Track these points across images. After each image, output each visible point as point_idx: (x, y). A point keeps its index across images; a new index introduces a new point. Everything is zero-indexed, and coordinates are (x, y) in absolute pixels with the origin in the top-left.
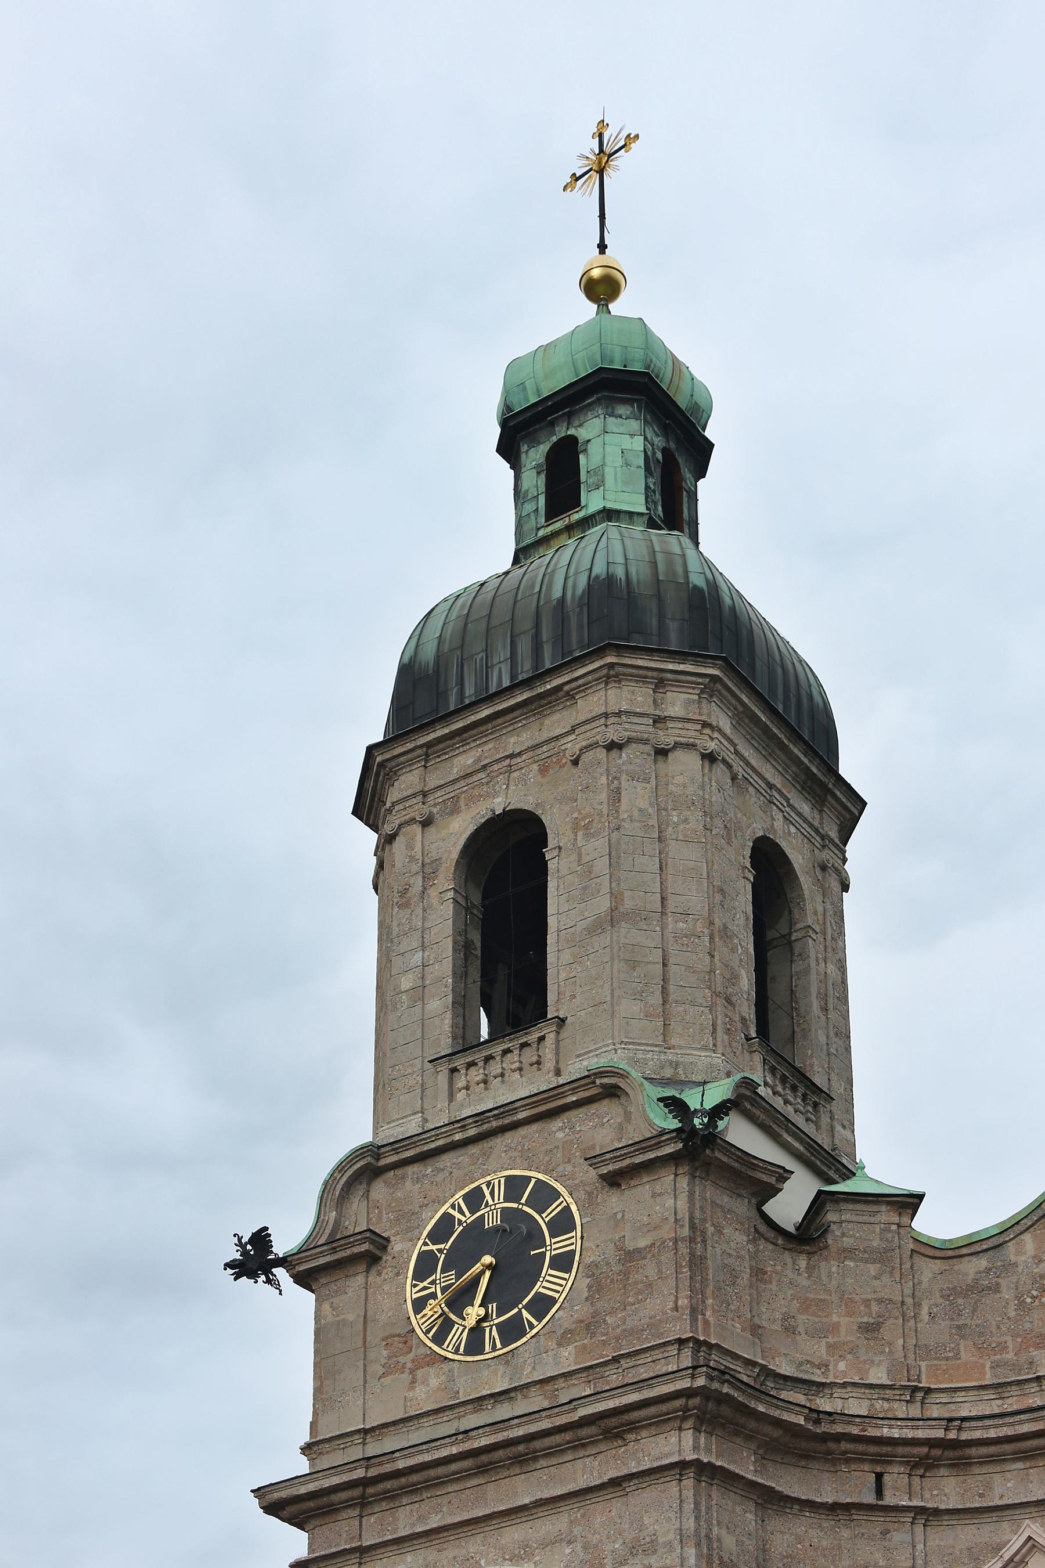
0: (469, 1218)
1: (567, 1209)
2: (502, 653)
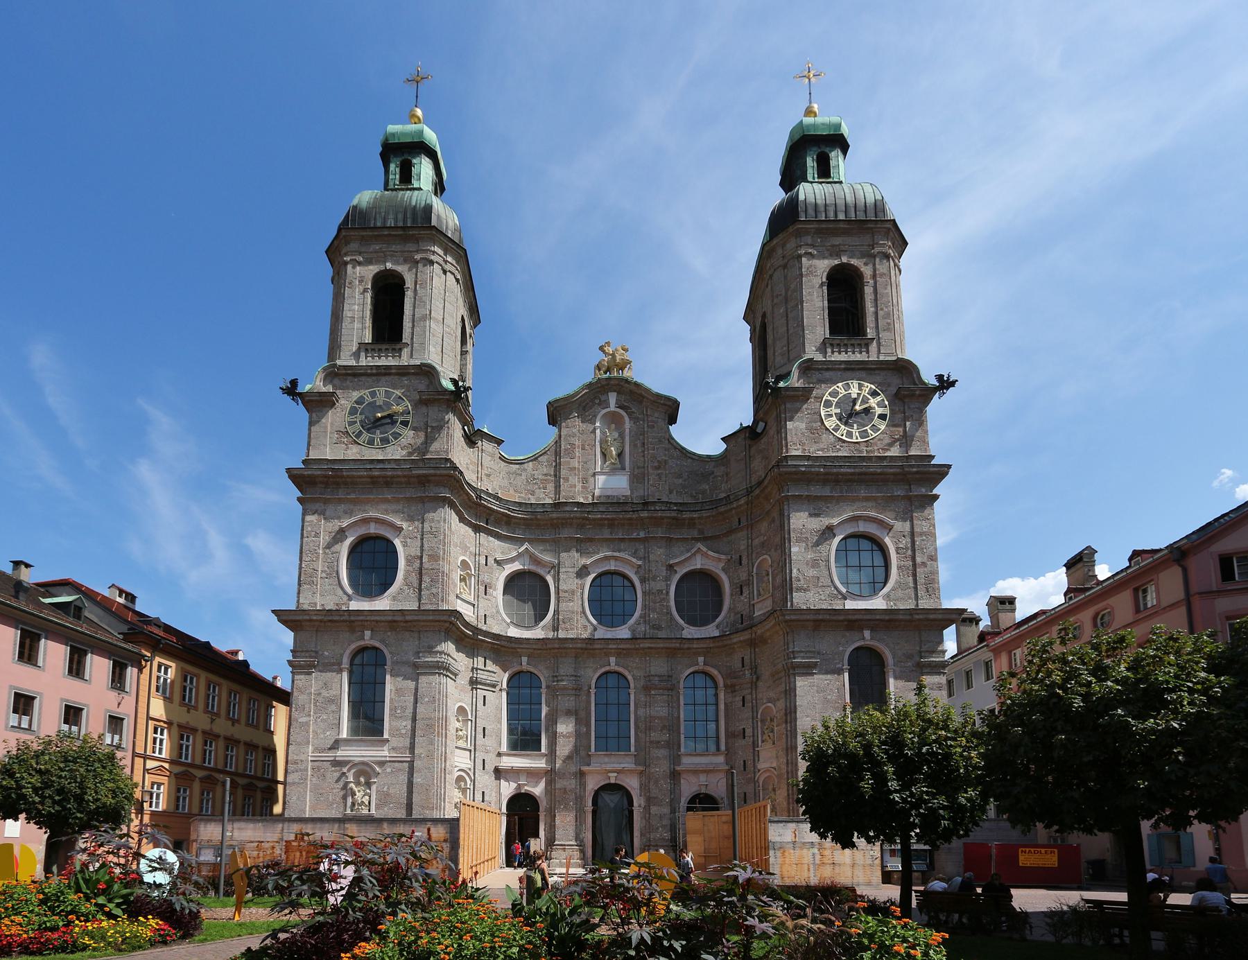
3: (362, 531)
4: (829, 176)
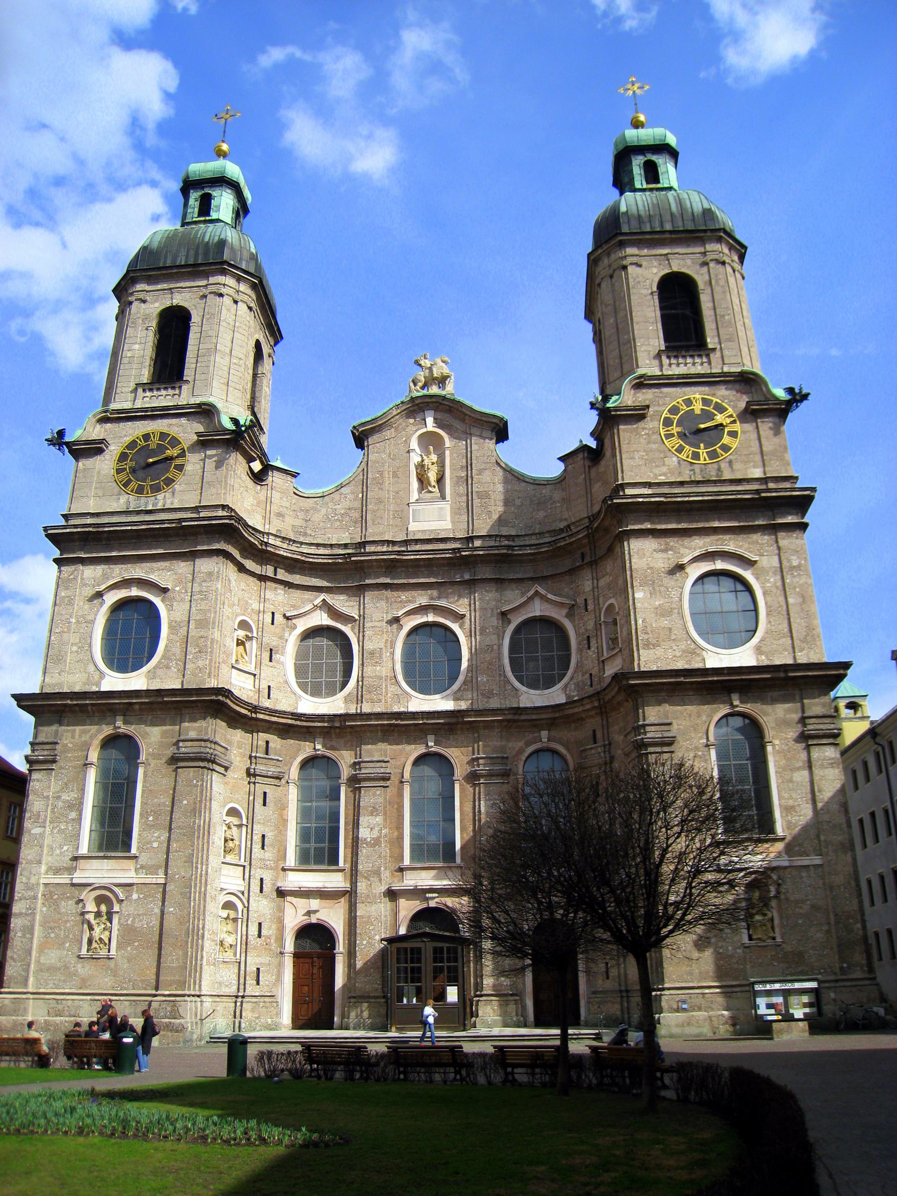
3: (122, 594)
4: (658, 182)
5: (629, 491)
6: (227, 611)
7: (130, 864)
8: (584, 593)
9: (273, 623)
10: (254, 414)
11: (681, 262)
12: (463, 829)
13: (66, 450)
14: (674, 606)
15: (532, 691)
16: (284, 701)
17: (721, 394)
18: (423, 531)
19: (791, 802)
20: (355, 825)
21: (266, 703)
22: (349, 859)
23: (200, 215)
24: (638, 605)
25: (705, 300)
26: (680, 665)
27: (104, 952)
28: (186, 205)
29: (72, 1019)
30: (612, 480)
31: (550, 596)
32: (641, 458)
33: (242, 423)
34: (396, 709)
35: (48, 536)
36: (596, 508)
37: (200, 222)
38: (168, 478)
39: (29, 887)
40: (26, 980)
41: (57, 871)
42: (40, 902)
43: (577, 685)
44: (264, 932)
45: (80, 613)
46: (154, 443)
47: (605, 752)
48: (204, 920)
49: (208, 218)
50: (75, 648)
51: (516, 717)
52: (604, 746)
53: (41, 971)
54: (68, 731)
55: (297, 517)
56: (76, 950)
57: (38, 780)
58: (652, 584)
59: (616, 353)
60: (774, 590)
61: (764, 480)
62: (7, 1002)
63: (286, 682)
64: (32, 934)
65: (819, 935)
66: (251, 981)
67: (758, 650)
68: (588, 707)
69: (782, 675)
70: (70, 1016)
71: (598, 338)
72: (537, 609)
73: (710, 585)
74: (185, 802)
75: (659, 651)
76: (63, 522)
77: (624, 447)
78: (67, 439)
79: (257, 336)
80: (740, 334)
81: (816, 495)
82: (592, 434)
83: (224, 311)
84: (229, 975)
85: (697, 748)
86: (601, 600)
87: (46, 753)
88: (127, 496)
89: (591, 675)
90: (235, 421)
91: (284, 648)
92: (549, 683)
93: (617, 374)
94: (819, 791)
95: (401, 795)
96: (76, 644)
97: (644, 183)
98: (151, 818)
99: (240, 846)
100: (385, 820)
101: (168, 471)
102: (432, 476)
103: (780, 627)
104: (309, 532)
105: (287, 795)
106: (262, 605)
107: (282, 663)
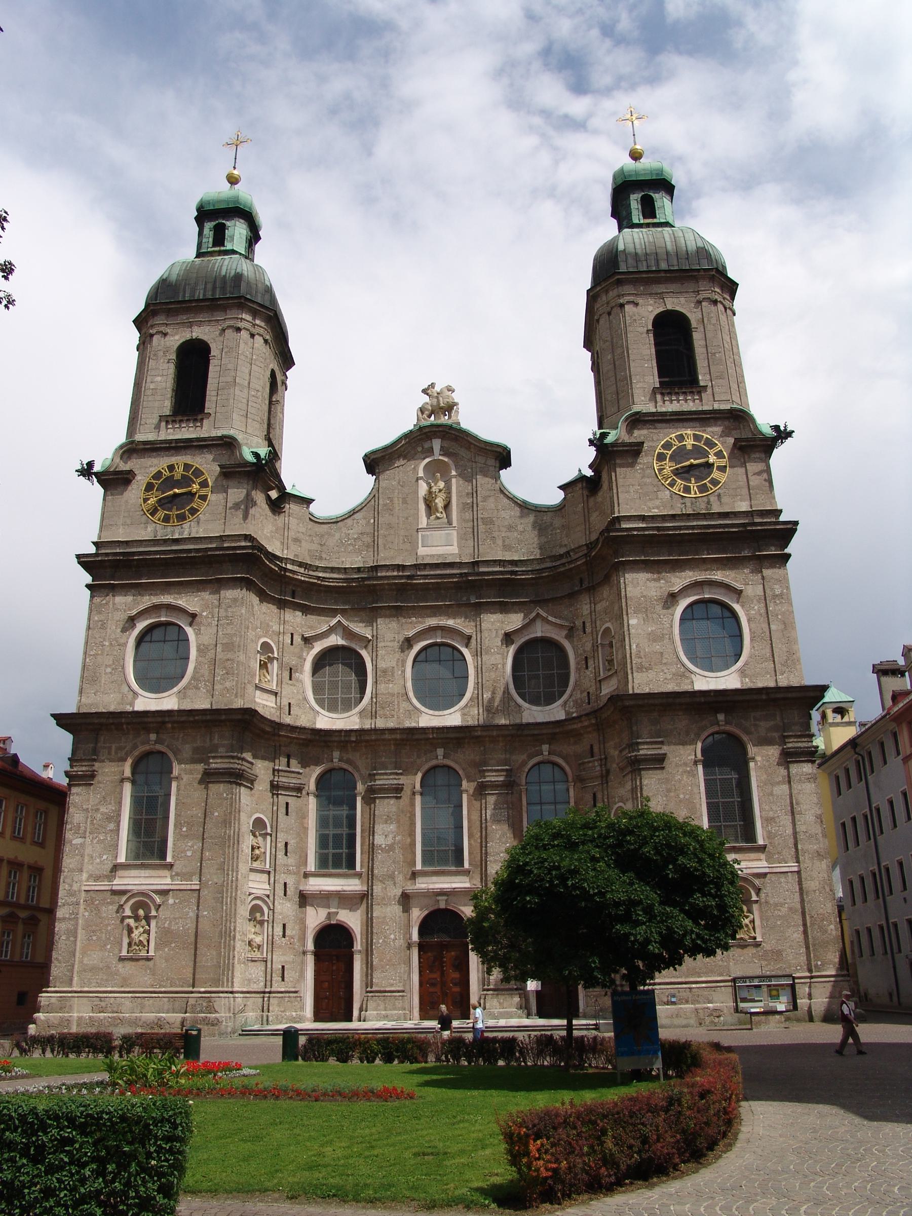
0: (168, 474)
1: (206, 479)
2: (201, 286)
4: (655, 217)
5: (625, 525)
6: (251, 634)
7: (166, 873)
8: (582, 616)
9: (292, 644)
10: (271, 444)
11: (675, 300)
12: (470, 836)
13: (95, 480)
14: (665, 632)
15: (534, 708)
16: (303, 716)
17: (711, 433)
18: (431, 556)
19: (771, 814)
20: (371, 831)
21: (287, 720)
22: (366, 864)
23: (214, 245)
24: (632, 631)
25: (697, 337)
26: (670, 687)
27: (143, 954)
28: (200, 234)
29: (115, 1015)
30: (609, 511)
31: (550, 618)
32: (636, 492)
33: (262, 456)
34: (408, 724)
35: (79, 563)
36: (594, 537)
37: (214, 252)
38: (192, 508)
39: (71, 894)
40: (71, 980)
41: (97, 878)
42: (82, 907)
43: (575, 702)
44: (288, 932)
45: (113, 636)
46: (179, 472)
47: (601, 766)
48: (235, 922)
49: (222, 248)
50: (109, 670)
51: (519, 733)
52: (601, 760)
53: (85, 971)
54: (105, 748)
55: (312, 541)
56: (116, 951)
57: (77, 794)
58: (645, 611)
59: (614, 388)
60: (758, 617)
61: (750, 514)
62: (53, 1000)
63: (305, 699)
64: (76, 937)
65: (795, 935)
66: (277, 978)
67: (742, 672)
68: (586, 724)
69: (764, 697)
70: (113, 1012)
71: (596, 367)
72: (539, 631)
73: (699, 611)
74: (216, 814)
75: (651, 674)
76: (92, 550)
77: (620, 481)
78: (97, 468)
79: (271, 366)
80: (730, 371)
81: (798, 527)
82: (590, 466)
83: (242, 345)
84: (257, 971)
85: (685, 764)
86: (598, 623)
87: (84, 769)
88: (154, 525)
89: (588, 693)
90: (256, 455)
91: (302, 666)
92: (549, 699)
93: (615, 409)
94: (797, 804)
95: (413, 805)
96: (110, 666)
97: (641, 217)
98: (184, 829)
99: (265, 853)
100: (398, 827)
101: (192, 501)
102: (440, 502)
103: (763, 652)
104: (324, 556)
105: (307, 805)
106: (282, 627)
107: (301, 681)
